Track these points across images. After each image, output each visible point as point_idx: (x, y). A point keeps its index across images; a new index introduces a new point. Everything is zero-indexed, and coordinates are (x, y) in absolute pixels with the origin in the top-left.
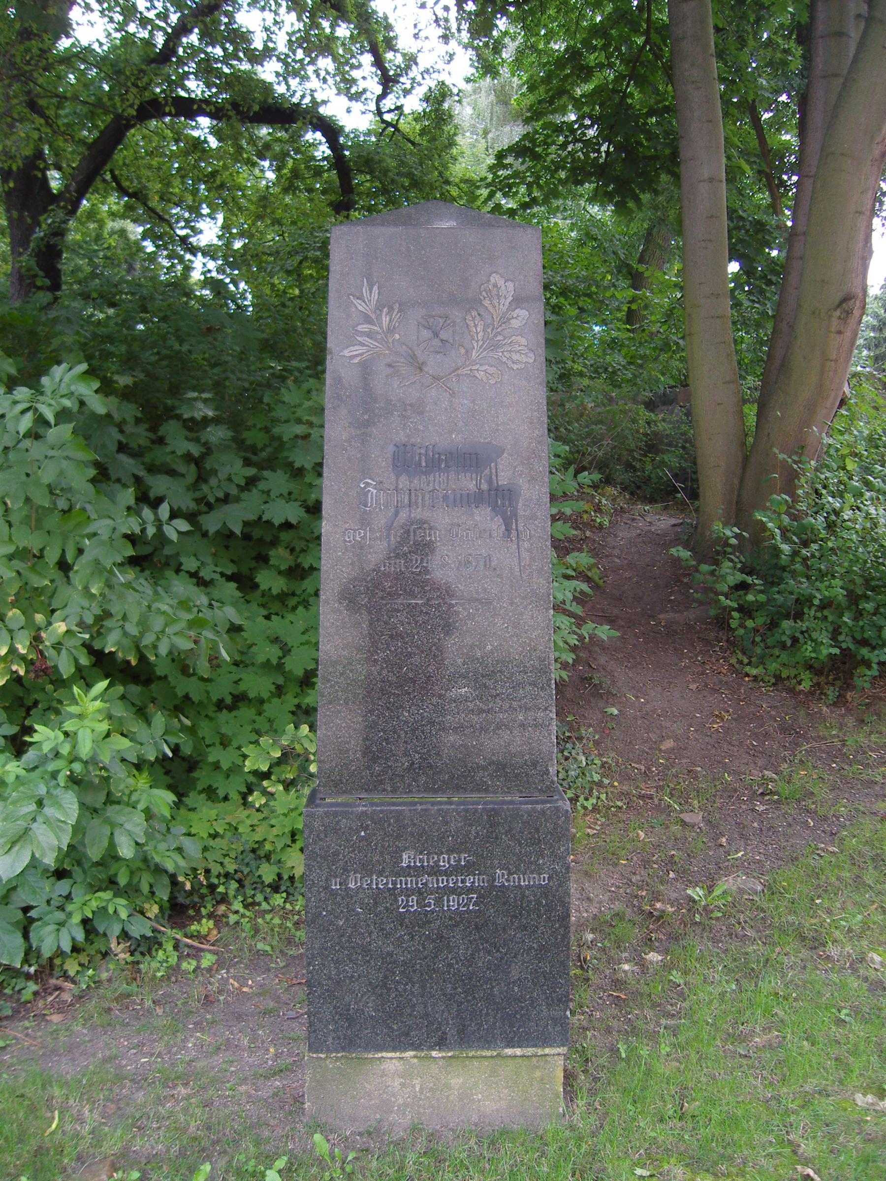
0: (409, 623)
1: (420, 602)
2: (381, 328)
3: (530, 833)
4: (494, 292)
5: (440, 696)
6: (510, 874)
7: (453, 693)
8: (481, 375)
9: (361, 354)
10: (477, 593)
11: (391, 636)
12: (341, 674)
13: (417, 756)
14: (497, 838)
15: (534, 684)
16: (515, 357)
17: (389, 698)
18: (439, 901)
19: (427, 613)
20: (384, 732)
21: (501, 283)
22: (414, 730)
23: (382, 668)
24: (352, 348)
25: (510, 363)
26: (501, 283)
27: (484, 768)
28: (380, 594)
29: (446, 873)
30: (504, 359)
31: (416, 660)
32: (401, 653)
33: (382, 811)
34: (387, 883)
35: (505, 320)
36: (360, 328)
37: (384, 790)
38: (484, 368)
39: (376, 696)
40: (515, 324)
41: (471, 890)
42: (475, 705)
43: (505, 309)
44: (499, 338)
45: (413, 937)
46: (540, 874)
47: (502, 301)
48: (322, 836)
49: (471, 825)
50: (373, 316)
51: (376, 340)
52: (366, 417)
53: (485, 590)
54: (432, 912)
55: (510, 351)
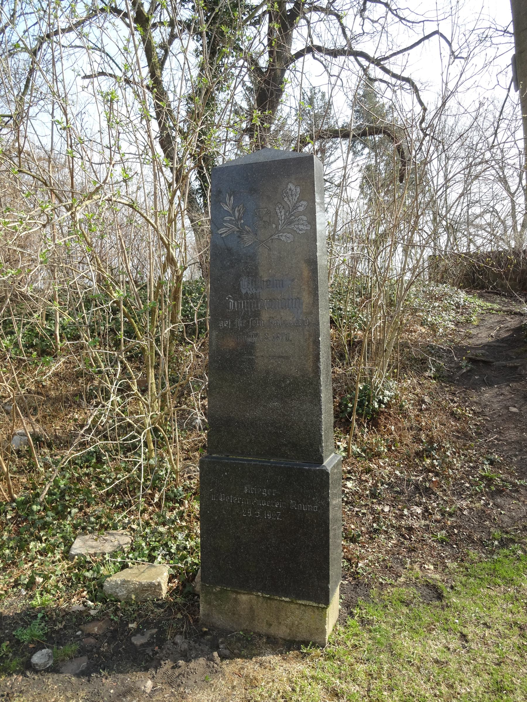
4: (290, 193)
5: (264, 406)
6: (298, 503)
7: (270, 405)
8: (283, 238)
10: (282, 353)
11: (241, 375)
13: (253, 436)
15: (311, 402)
16: (301, 227)
18: (262, 513)
20: (238, 422)
21: (293, 188)
25: (298, 231)
26: (293, 188)
27: (286, 445)
30: (295, 229)
33: (235, 463)
34: (237, 501)
35: (295, 207)
40: (301, 209)
41: (278, 509)
44: (293, 217)
46: (313, 506)
48: (208, 473)
50: (231, 212)
53: (286, 351)
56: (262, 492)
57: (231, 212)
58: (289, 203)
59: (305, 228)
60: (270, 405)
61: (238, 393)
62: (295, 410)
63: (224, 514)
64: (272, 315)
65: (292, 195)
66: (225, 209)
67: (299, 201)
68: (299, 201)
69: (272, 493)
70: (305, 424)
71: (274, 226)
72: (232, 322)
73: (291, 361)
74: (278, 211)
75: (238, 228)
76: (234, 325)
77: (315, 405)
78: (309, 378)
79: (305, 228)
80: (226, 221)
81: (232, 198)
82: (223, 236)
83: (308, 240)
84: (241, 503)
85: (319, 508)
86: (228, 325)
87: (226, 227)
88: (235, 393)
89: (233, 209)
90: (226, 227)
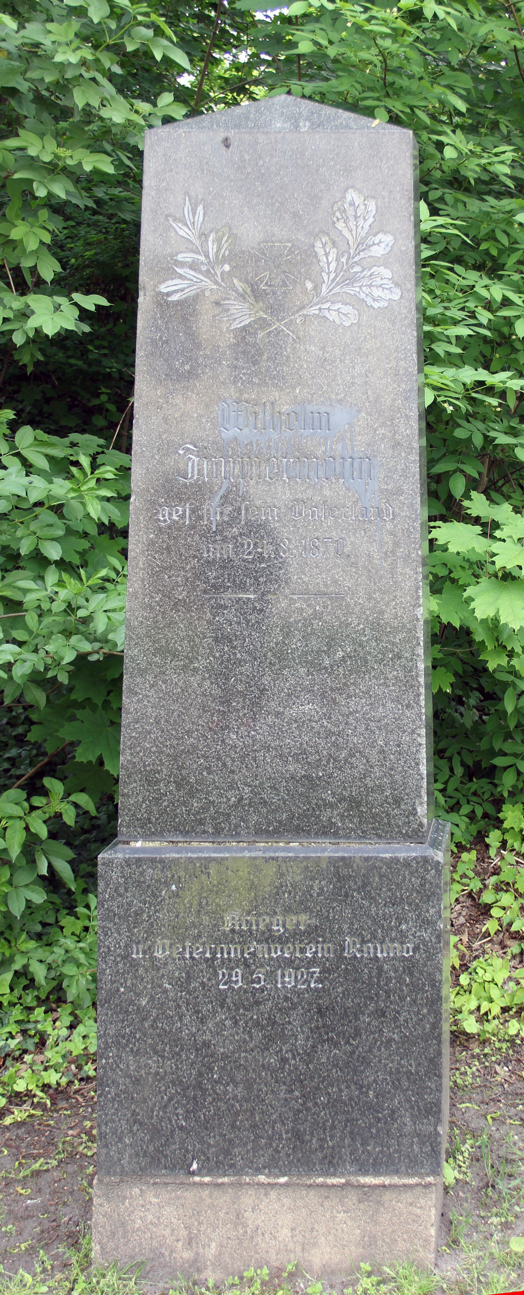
0: (239, 623)
1: (252, 596)
2: (207, 256)
3: (390, 890)
4: (351, 212)
5: (278, 714)
6: (363, 942)
7: (293, 712)
8: (332, 316)
9: (182, 290)
10: (326, 585)
11: (216, 640)
12: (152, 686)
13: (247, 789)
14: (346, 895)
15: (397, 700)
16: (377, 292)
17: (212, 715)
18: (271, 975)
19: (261, 610)
20: (205, 757)
21: (358, 200)
22: (243, 758)
23: (204, 679)
24: (170, 283)
25: (369, 301)
26: (358, 200)
27: (332, 806)
28: (203, 586)
29: (282, 940)
30: (363, 296)
31: (246, 669)
32: (229, 660)
34: (204, 952)
35: (363, 245)
36: (180, 257)
37: (204, 832)
38: (336, 307)
39: (196, 713)
40: (378, 251)
41: (313, 962)
42: (322, 726)
43: (363, 234)
44: (357, 269)
45: (236, 1023)
46: (402, 943)
47: (361, 222)
48: (122, 890)
49: (313, 879)
51: (200, 272)
52: (187, 367)
53: (335, 582)
54: (262, 990)
55: (370, 286)
57: (197, 242)
58: (346, 233)
59: (387, 295)
60: (293, 712)
61: (207, 684)
62: (356, 719)
63: (166, 991)
64: (299, 496)
65: (356, 217)
66: (181, 233)
67: (374, 231)
68: (374, 231)
69: (298, 924)
70: (382, 752)
71: (309, 285)
72: (193, 511)
73: (348, 606)
74: (321, 252)
75: (216, 283)
76: (200, 518)
77: (408, 706)
78: (394, 644)
79: (387, 295)
80: (182, 264)
82: (174, 298)
83: (394, 323)
84: (214, 958)
85: (416, 949)
86: (183, 516)
87: (181, 277)
88: (200, 686)
89: (203, 236)
90: (181, 277)
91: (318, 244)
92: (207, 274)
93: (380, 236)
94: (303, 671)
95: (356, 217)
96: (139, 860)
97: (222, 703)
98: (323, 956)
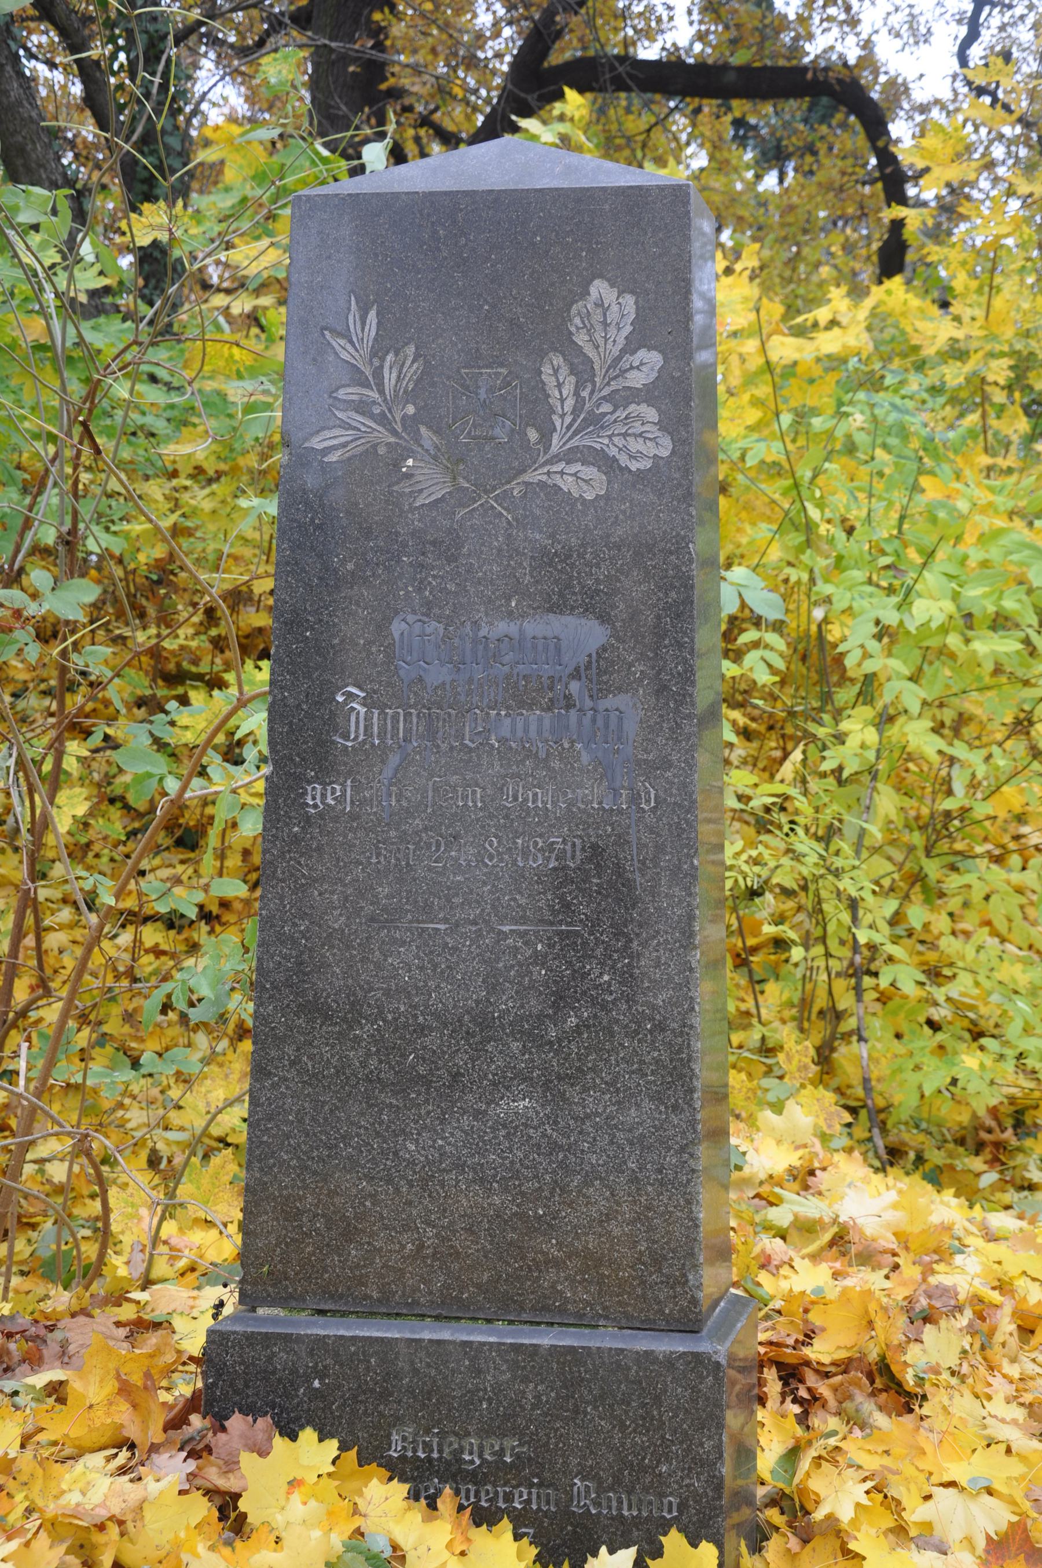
0: (422, 968)
1: (442, 927)
2: (382, 392)
3: (644, 1405)
7: (502, 1109)
8: (567, 484)
9: (344, 445)
12: (293, 1063)
13: (430, 1232)
14: (576, 1412)
15: (658, 1098)
16: (635, 445)
17: (380, 1112)
19: (455, 949)
22: (424, 1182)
23: (368, 1054)
24: (327, 434)
25: (624, 460)
27: (557, 1264)
28: (369, 909)
30: (613, 451)
31: (432, 1040)
32: (406, 1026)
33: (354, 1339)
36: (341, 394)
39: (356, 1108)
42: (544, 1135)
43: (615, 351)
47: (612, 332)
49: (525, 1380)
50: (368, 372)
51: (372, 417)
52: (350, 566)
55: (625, 435)
56: (461, 1450)
58: (589, 351)
59: (650, 449)
60: (502, 1109)
61: (373, 1063)
62: (597, 1127)
67: (631, 347)
68: (631, 347)
69: (502, 1452)
74: (550, 381)
75: (394, 432)
77: (675, 1108)
78: (654, 1007)
79: (650, 449)
81: (372, 316)
82: (333, 457)
88: (364, 1065)
91: (547, 369)
92: (382, 420)
93: (642, 354)
94: (516, 1046)
95: (605, 324)
96: (267, 1336)
97: (395, 1093)
98: (539, 1509)
